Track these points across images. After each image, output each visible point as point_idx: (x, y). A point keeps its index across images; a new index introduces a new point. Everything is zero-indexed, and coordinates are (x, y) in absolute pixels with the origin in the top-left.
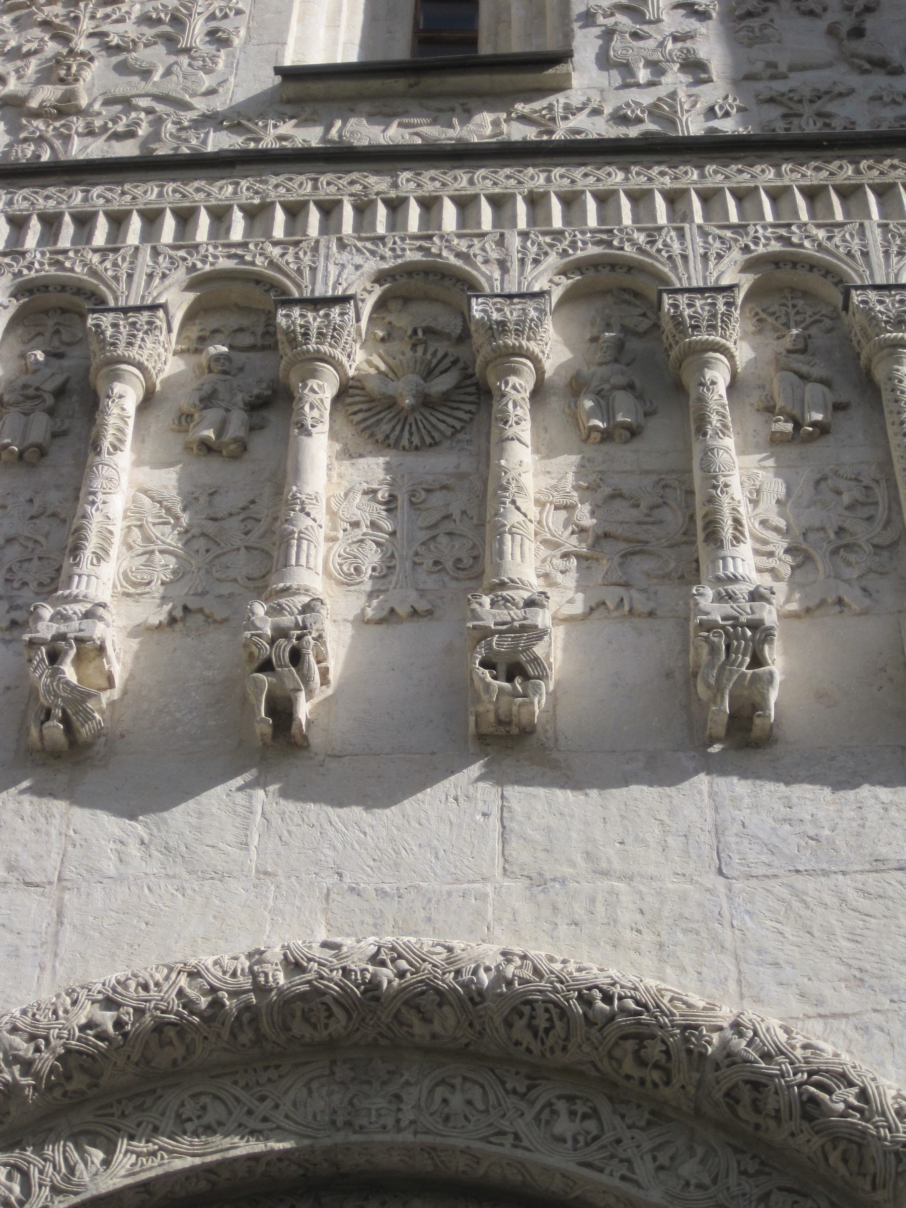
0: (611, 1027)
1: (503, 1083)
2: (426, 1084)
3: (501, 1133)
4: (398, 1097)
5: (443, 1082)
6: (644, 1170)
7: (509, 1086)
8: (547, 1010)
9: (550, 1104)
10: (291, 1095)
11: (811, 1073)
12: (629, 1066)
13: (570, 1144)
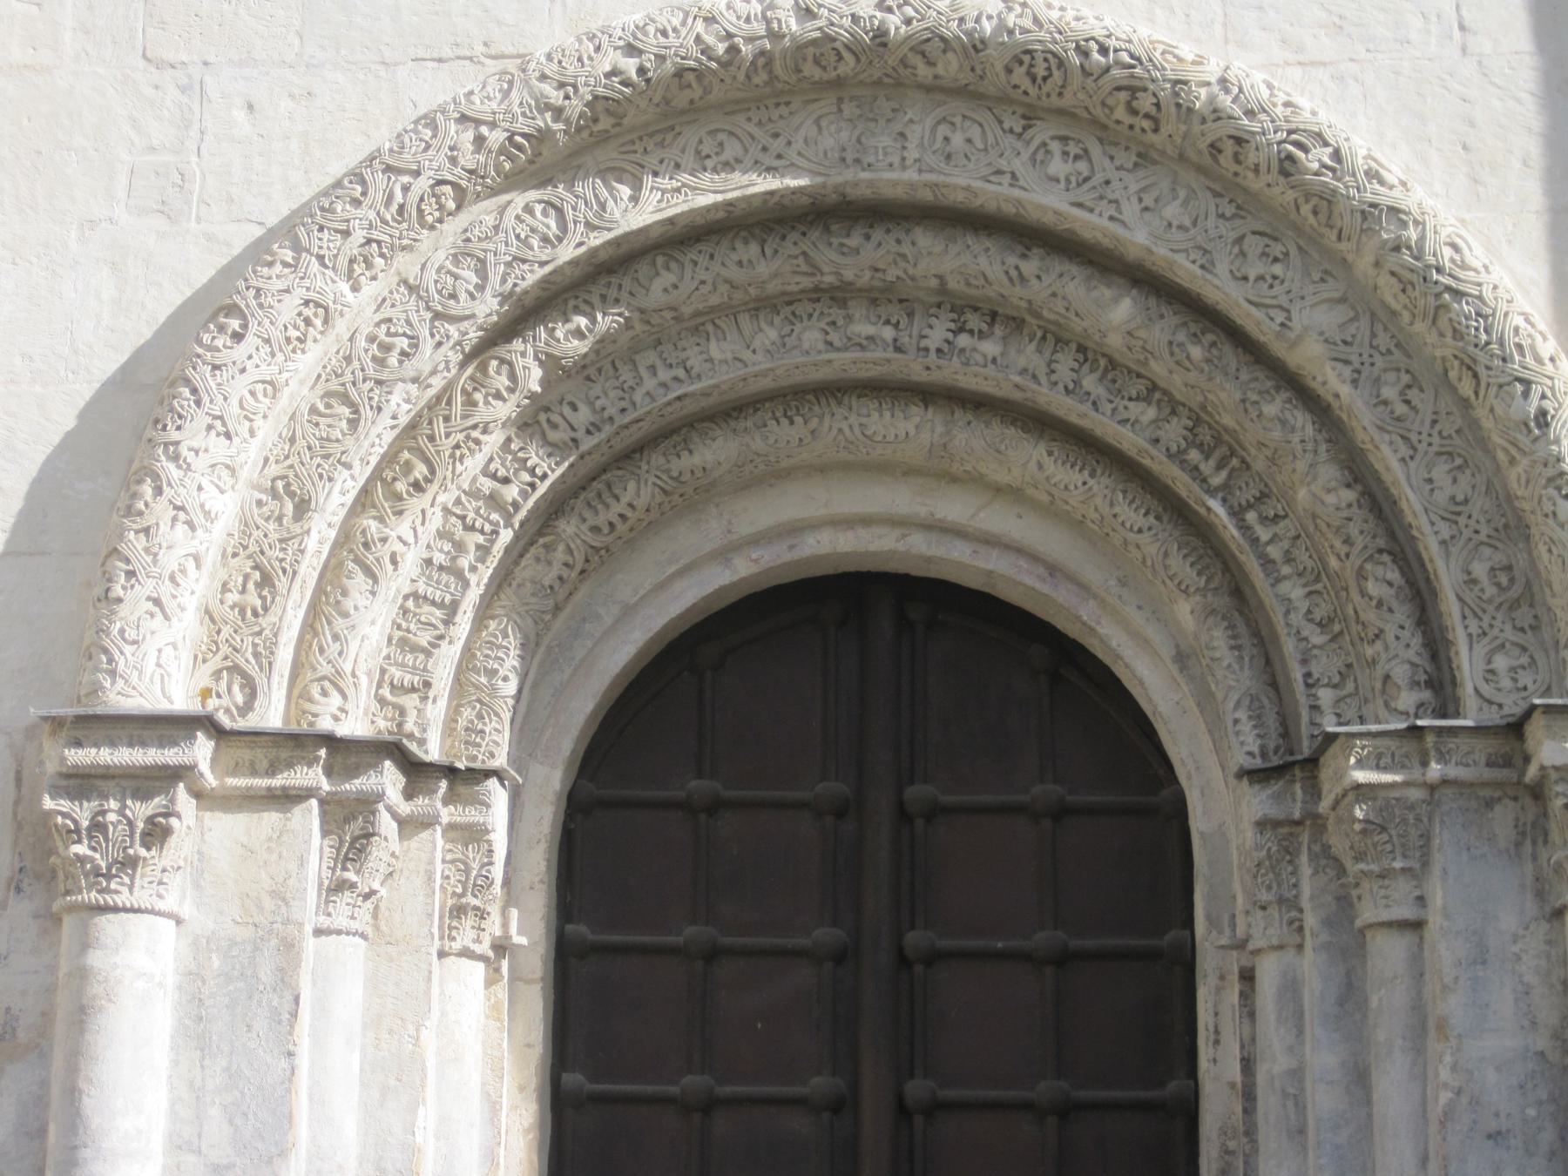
0: (1106, 78)
1: (1000, 122)
2: (929, 122)
3: (999, 172)
4: (902, 135)
6: (1130, 211)
7: (1006, 126)
8: (1046, 60)
9: (1044, 144)
10: (802, 132)
11: (1290, 132)
12: (1120, 113)
13: (1062, 185)
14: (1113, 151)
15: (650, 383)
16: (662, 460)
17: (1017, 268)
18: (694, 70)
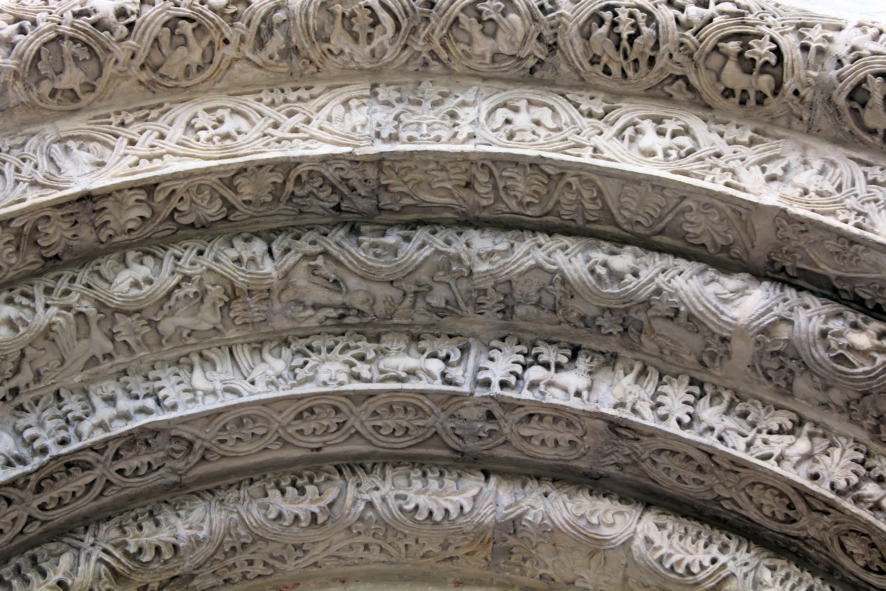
0: (709, 28)
1: (577, 106)
2: (485, 106)
4: (453, 115)
5: (504, 105)
7: (583, 107)
8: (631, 15)
10: (326, 111)
12: (733, 75)
13: (660, 156)
14: (721, 128)
15: (104, 412)
16: (115, 533)
17: (605, 264)
18: (190, 20)
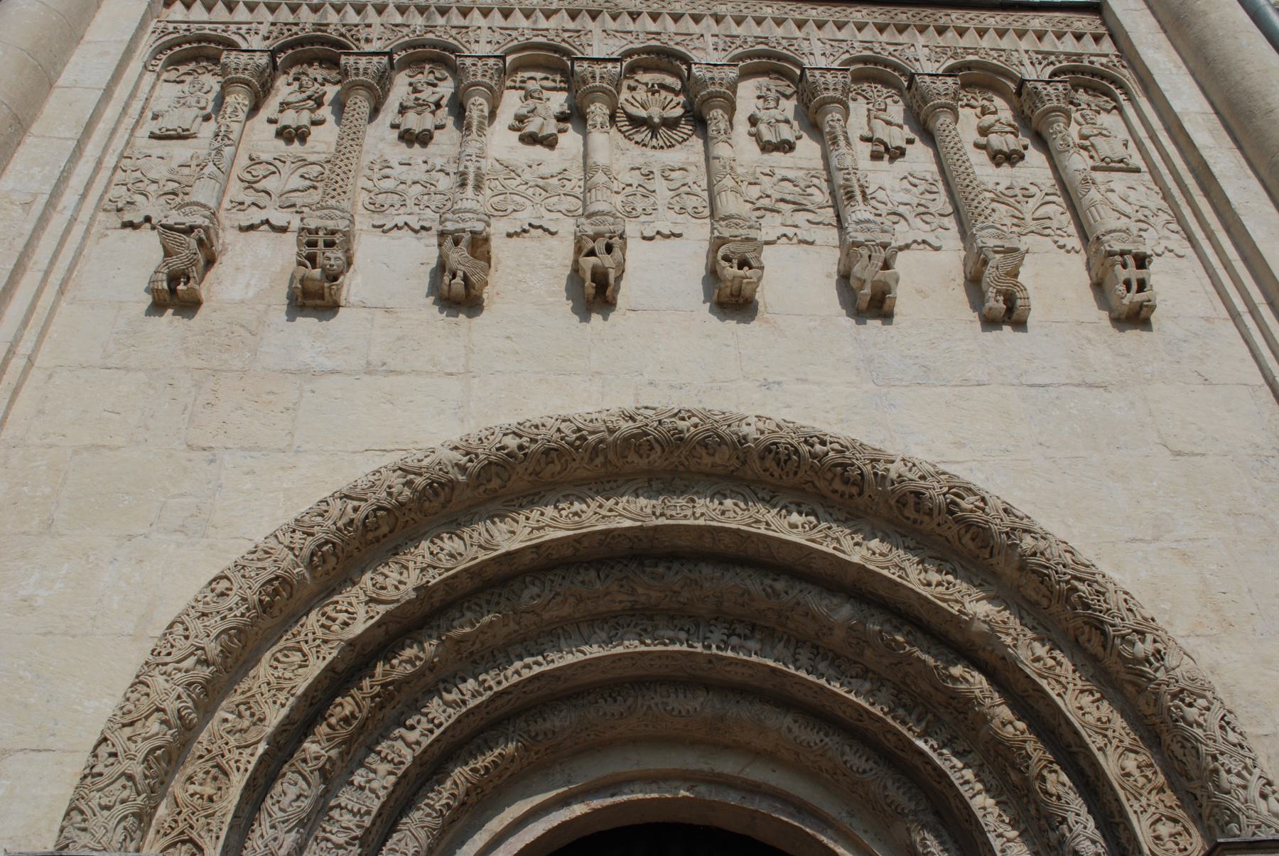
3: (758, 521)
5: (719, 492)
11: (950, 488)
12: (837, 485)
14: (831, 510)
16: (523, 725)
17: (771, 587)
18: (556, 450)
